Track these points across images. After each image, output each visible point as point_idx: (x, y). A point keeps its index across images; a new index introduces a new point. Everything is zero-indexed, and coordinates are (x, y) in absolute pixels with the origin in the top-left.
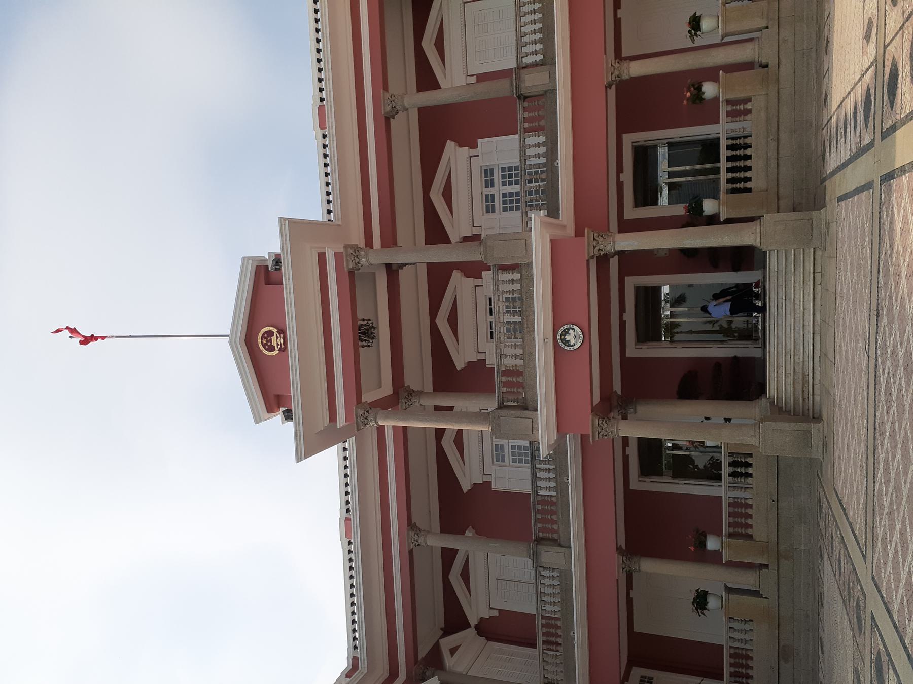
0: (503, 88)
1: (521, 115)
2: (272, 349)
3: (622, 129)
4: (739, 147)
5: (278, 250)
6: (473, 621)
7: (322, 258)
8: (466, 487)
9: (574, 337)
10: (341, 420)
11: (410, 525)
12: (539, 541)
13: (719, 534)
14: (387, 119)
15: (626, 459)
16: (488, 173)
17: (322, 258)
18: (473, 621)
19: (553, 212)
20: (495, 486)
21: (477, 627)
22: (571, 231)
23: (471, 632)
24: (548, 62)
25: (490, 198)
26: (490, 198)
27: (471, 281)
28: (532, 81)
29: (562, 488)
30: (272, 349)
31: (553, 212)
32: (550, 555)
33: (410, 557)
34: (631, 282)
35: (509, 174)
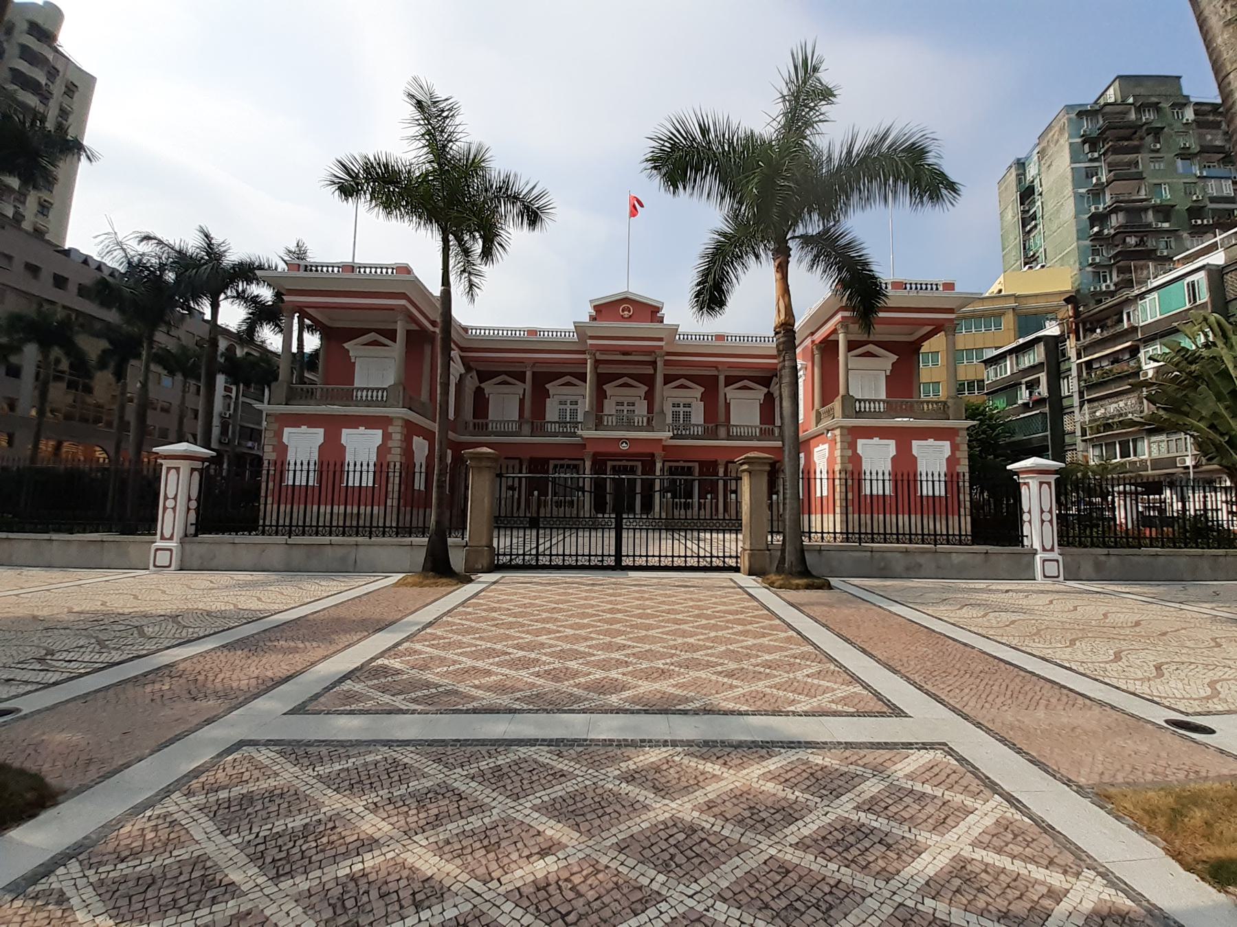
0: (722, 418)
1: (710, 425)
2: (623, 311)
3: (701, 463)
4: (687, 506)
5: (665, 322)
6: (483, 385)
7: (661, 339)
8: (547, 386)
9: (624, 447)
10: (590, 342)
11: (536, 362)
12: (532, 423)
13: (539, 495)
14: (716, 367)
15: (563, 459)
16: (689, 406)
17: (661, 339)
18: (483, 385)
19: (672, 438)
20: (548, 400)
21: (479, 387)
22: (664, 443)
23: (477, 383)
24: (729, 437)
25: (679, 406)
26: (679, 406)
27: (643, 395)
28: (722, 431)
29: (555, 435)
30: (623, 311)
31: (672, 438)
32: (526, 428)
33: (521, 362)
34: (639, 464)
35: (687, 415)
